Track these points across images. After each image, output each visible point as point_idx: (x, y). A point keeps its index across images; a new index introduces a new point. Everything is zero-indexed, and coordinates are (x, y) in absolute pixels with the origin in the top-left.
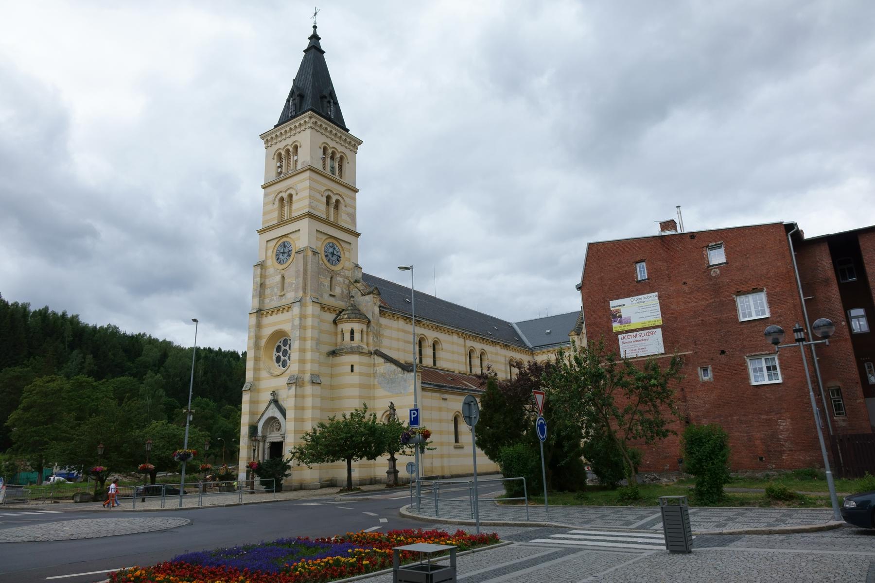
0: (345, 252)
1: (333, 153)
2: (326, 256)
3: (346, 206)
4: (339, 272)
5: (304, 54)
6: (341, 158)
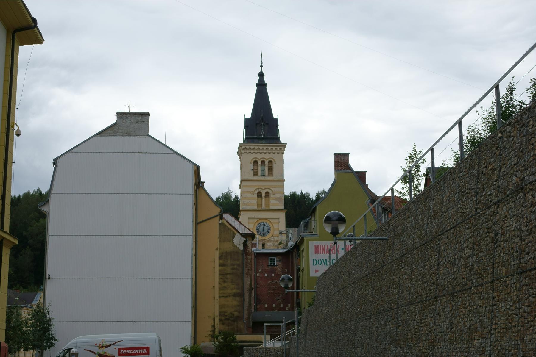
0: (273, 225)
3: (274, 194)
4: (269, 239)
6: (270, 162)
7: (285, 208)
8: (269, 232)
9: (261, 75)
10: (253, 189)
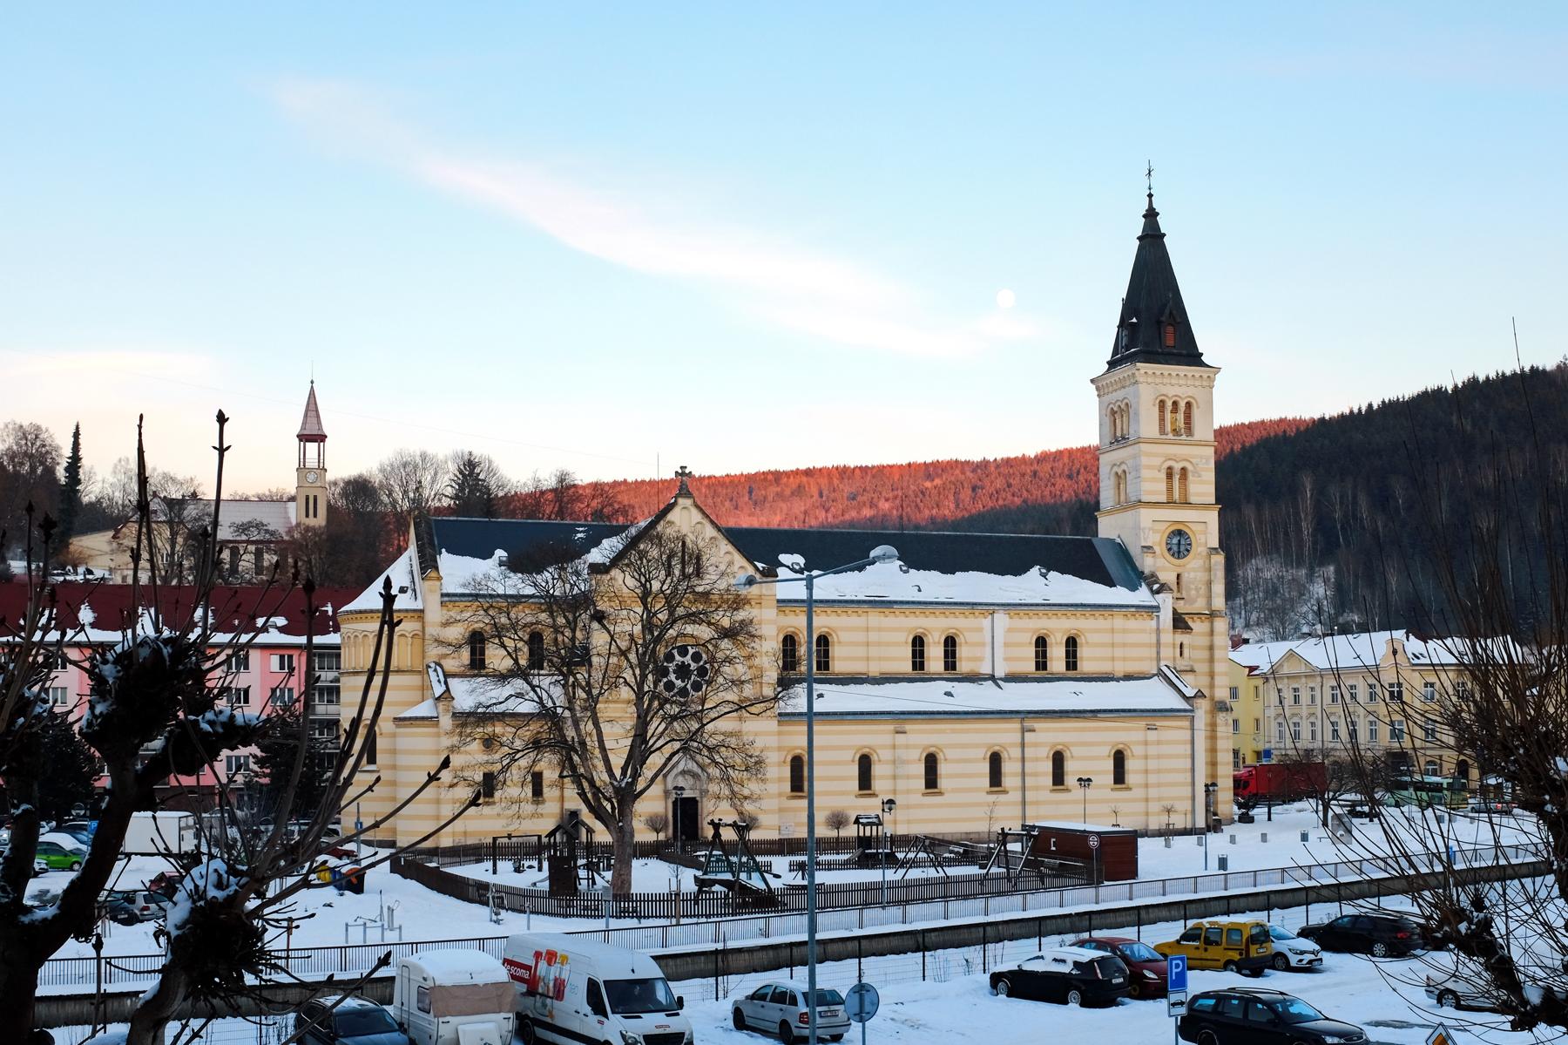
1: (1175, 404)
2: (1169, 550)
5: (1138, 242)
6: (1189, 405)
7: (1218, 500)
8: (1188, 551)
9: (1151, 215)
10: (1157, 461)
